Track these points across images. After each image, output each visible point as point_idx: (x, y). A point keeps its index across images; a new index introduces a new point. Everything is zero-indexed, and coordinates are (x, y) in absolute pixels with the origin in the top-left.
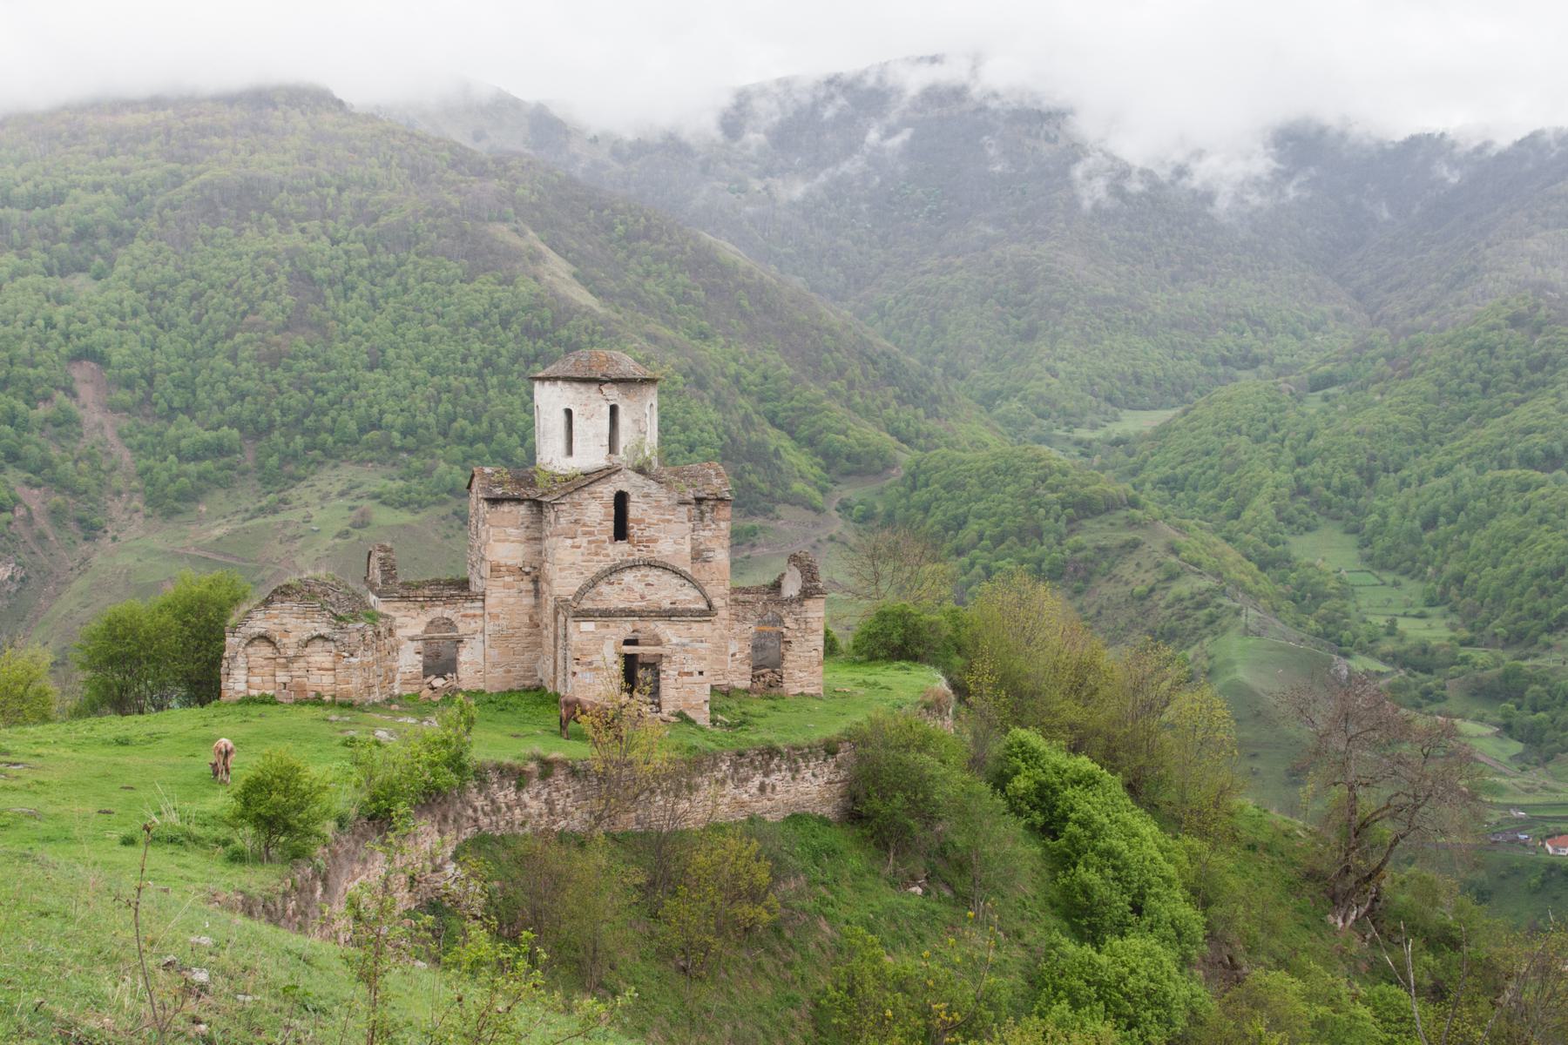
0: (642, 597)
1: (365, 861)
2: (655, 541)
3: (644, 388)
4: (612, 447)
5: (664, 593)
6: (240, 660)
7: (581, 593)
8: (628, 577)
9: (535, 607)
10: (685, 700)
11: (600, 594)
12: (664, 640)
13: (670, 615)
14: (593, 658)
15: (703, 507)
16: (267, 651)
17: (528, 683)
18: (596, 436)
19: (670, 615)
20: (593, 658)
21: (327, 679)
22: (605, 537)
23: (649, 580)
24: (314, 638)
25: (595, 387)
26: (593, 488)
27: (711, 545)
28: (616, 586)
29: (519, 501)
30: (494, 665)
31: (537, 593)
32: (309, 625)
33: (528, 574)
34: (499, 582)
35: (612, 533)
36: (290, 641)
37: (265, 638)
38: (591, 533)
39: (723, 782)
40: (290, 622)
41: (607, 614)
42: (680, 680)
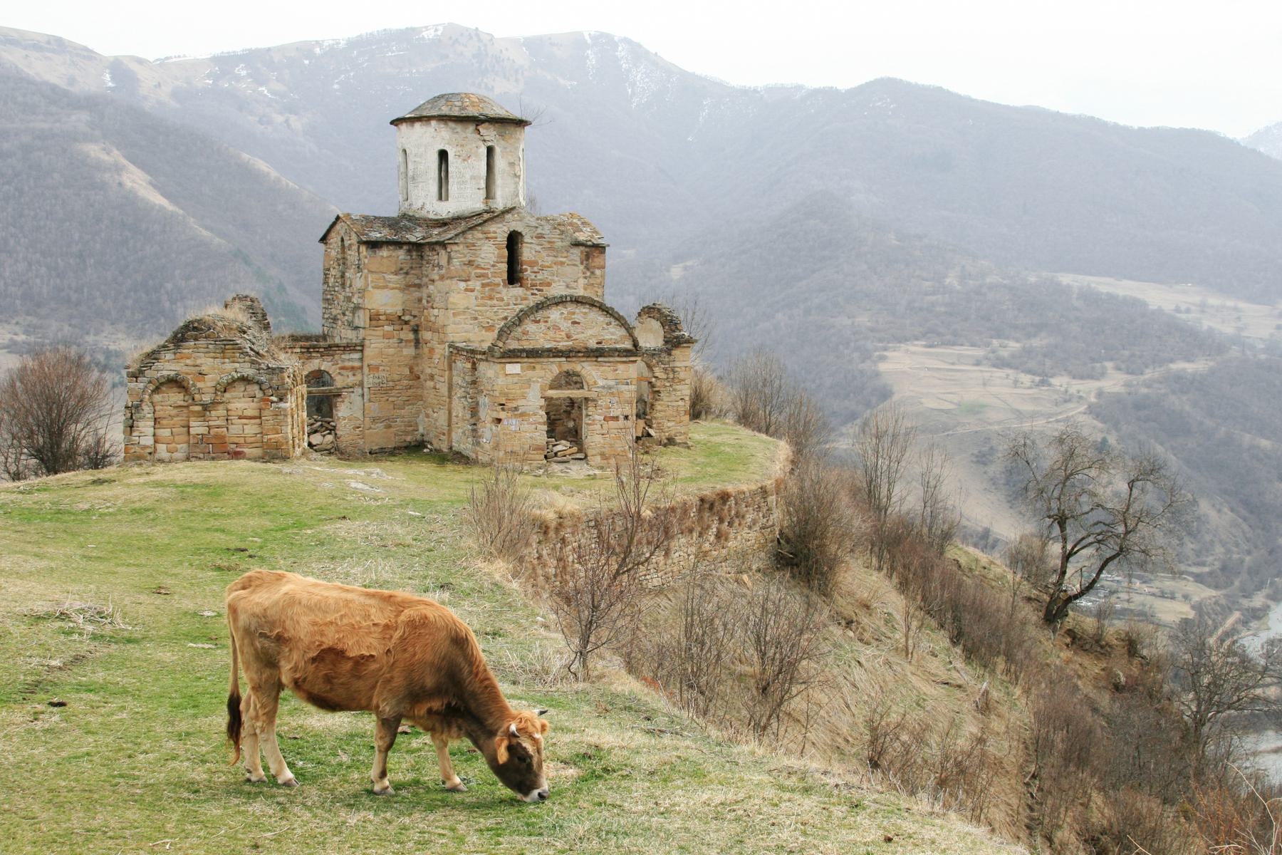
0: (568, 337)
2: (549, 284)
5: (590, 332)
7: (502, 333)
8: (555, 314)
9: (415, 357)
10: (611, 446)
13: (597, 354)
14: (520, 402)
16: (176, 397)
17: (409, 438)
18: (473, 178)
19: (597, 354)
20: (520, 402)
21: (251, 429)
22: (498, 280)
23: (577, 318)
24: (234, 381)
25: (471, 128)
28: (542, 325)
29: (398, 244)
30: (374, 420)
32: (229, 366)
33: (406, 323)
34: (379, 332)
37: (176, 382)
41: (534, 354)
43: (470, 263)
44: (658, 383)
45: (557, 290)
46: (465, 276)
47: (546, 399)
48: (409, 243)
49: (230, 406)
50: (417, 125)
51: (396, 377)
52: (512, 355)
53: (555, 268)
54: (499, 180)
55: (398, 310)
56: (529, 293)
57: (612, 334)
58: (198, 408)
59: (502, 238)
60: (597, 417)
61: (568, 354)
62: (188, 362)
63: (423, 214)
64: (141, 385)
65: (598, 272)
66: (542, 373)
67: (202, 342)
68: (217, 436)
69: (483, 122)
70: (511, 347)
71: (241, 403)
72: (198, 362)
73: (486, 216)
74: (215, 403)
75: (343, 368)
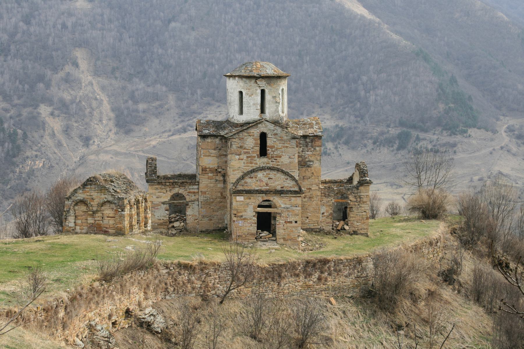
0: (267, 185)
1: (97, 303)
2: (280, 157)
3: (279, 81)
4: (263, 111)
5: (277, 183)
6: (72, 212)
8: (260, 175)
10: (288, 235)
11: (246, 183)
12: (278, 205)
13: (280, 193)
15: (308, 140)
16: (83, 208)
17: (220, 226)
18: (254, 104)
19: (280, 193)
20: (243, 214)
21: (112, 222)
22: (255, 155)
23: (271, 176)
24: (105, 202)
25: (253, 81)
26: (249, 131)
27: (311, 159)
28: (254, 179)
29: (216, 136)
30: (203, 217)
31: (225, 182)
32: (103, 196)
33: (220, 172)
35: (259, 153)
36: (95, 203)
37: (83, 202)
38: (248, 153)
39: (297, 275)
40: (95, 194)
41: (249, 192)
42: (285, 225)
43: (241, 147)
44: (351, 203)
46: (238, 153)
48: (220, 136)
49: (104, 212)
51: (214, 197)
53: (283, 149)
54: (267, 105)
55: (215, 166)
56: (270, 161)
57: (289, 184)
58: (91, 213)
60: (281, 221)
62: (88, 194)
63: (232, 120)
64: (70, 203)
66: (254, 201)
67: (93, 186)
68: (98, 224)
69: (259, 78)
70: (239, 189)
71: (108, 211)
72: (92, 194)
74: (97, 211)
75: (189, 192)
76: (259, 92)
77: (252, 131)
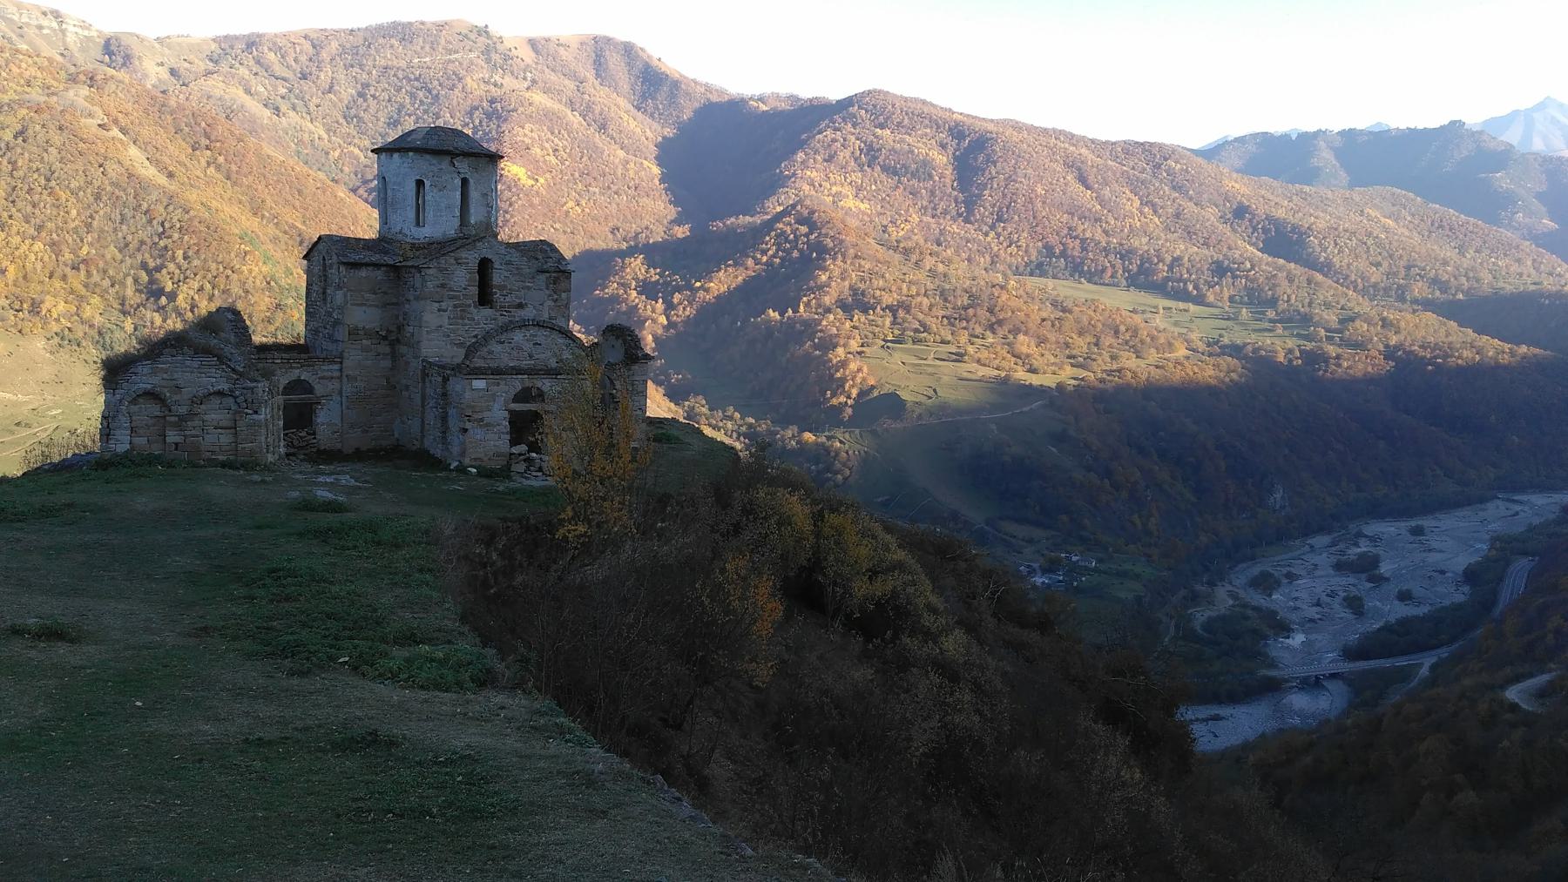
0: (531, 356)
7: (471, 351)
8: (518, 336)
14: (486, 414)
18: (448, 207)
29: (377, 266)
33: (385, 338)
37: (152, 395)
41: (497, 372)
45: (529, 313)
47: (511, 412)
49: (206, 417)
50: (396, 155)
52: (478, 373)
59: (474, 265)
61: (531, 372)
65: (564, 295)
73: (459, 243)
74: (192, 415)
76: (458, 182)
77: (463, 254)
